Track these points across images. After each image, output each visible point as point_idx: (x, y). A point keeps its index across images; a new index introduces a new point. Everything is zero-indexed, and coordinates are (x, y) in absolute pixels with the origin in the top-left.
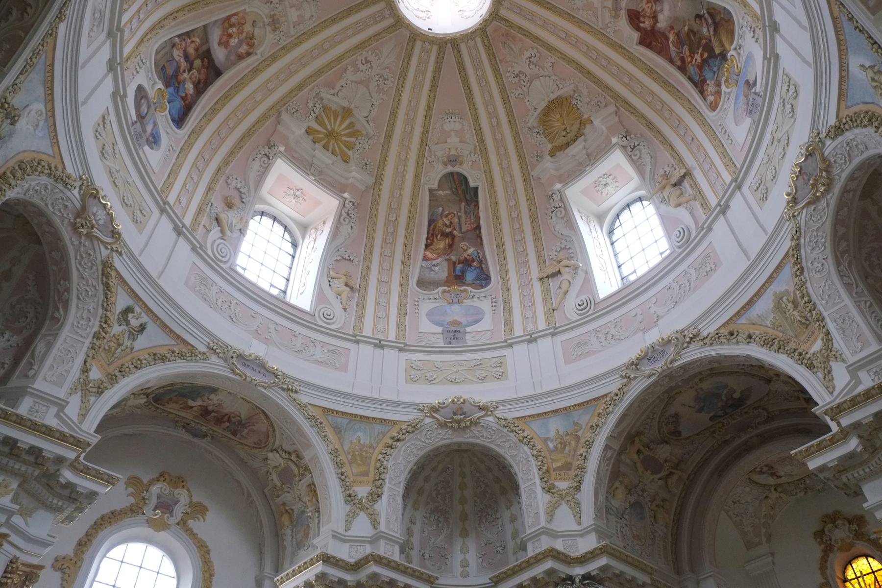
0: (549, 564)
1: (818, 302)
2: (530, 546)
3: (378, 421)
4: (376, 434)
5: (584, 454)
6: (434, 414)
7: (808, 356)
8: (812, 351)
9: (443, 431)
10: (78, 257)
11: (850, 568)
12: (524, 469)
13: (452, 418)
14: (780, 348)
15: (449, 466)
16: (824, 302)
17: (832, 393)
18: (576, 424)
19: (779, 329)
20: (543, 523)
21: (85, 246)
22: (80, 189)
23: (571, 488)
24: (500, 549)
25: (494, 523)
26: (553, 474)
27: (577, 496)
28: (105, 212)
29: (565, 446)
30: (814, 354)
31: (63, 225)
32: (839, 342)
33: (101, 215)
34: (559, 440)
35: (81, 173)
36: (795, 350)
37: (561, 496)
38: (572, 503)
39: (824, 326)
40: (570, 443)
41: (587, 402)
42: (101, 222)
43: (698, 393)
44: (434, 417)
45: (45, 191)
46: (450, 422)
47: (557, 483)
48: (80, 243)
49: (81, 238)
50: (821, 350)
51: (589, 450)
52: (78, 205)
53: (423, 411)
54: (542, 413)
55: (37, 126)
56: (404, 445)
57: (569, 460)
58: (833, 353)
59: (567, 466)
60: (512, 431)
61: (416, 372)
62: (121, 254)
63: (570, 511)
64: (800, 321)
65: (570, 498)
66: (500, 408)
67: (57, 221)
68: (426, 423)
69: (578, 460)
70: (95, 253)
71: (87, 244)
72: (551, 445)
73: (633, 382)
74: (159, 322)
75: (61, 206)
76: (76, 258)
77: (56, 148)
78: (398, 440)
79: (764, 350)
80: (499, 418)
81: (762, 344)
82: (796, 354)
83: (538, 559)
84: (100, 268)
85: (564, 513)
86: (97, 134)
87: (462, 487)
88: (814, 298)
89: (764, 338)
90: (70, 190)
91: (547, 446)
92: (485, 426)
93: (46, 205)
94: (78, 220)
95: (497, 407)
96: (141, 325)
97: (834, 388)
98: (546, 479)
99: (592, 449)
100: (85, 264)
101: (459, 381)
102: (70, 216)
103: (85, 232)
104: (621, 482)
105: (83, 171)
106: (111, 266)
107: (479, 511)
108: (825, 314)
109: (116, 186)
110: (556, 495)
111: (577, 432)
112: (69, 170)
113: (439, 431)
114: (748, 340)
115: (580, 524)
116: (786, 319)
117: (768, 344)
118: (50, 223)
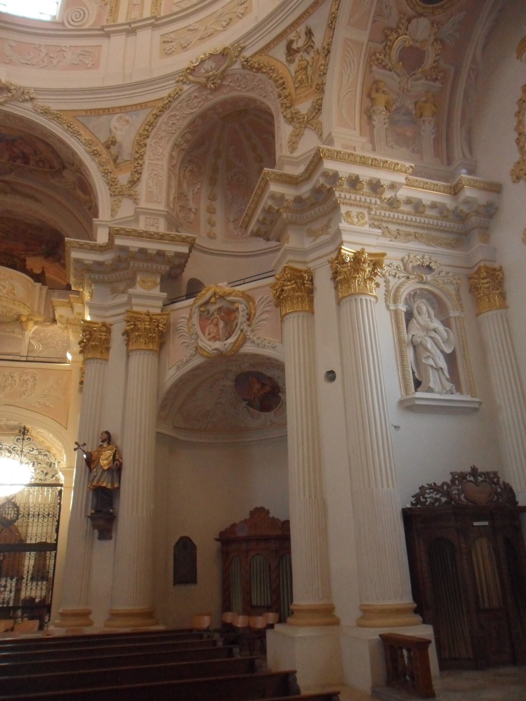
10: (239, 89)
21: (231, 82)
22: (184, 83)
28: (207, 61)
31: (212, 99)
33: (209, 65)
35: (174, 81)
42: (213, 65)
45: (176, 116)
48: (228, 85)
49: (224, 85)
52: (196, 87)
55: (127, 121)
62: (243, 48)
67: (208, 104)
70: (236, 74)
71: (229, 80)
74: (310, 11)
75: (195, 101)
76: (240, 91)
77: (149, 105)
84: (247, 72)
86: (168, 52)
90: (180, 95)
93: (191, 113)
94: (209, 86)
96: (306, 34)
100: (244, 84)
102: (204, 93)
103: (219, 81)
105: (172, 80)
106: (247, 61)
109: (212, 34)
112: (165, 94)
118: (213, 108)
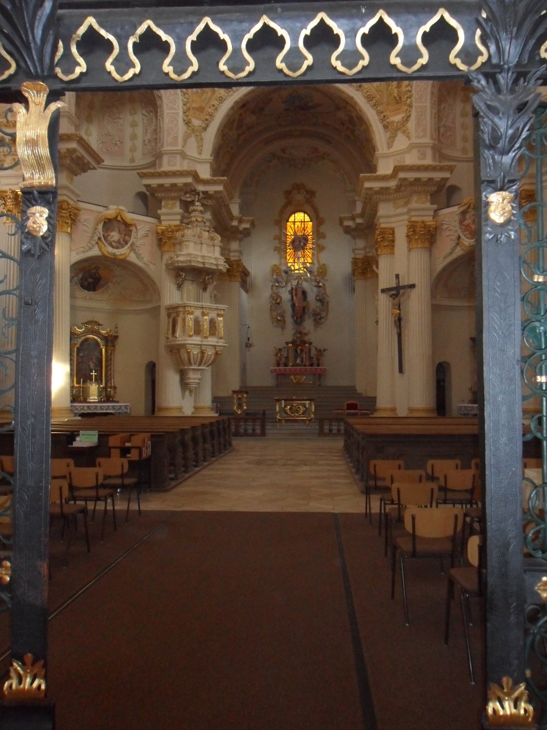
0: (189, 180)
1: (414, 95)
2: (165, 158)
5: (216, 106)
7: (388, 120)
8: (392, 119)
11: (293, 216)
12: (171, 98)
14: (375, 105)
16: (417, 97)
17: (389, 148)
19: (380, 93)
20: (179, 147)
23: (200, 126)
24: (118, 143)
25: (115, 121)
26: (192, 112)
27: (203, 134)
30: (392, 122)
32: (411, 125)
36: (382, 112)
37: (193, 130)
38: (199, 138)
39: (409, 111)
50: (398, 122)
51: (220, 104)
58: (404, 128)
59: (201, 109)
64: (395, 97)
65: (198, 134)
69: (210, 107)
79: (364, 100)
81: (366, 95)
82: (382, 115)
83: (181, 174)
85: (192, 142)
88: (413, 91)
89: (368, 93)
97: (392, 146)
98: (187, 114)
99: (222, 104)
108: (414, 104)
110: (190, 128)
114: (358, 88)
115: (200, 154)
116: (387, 90)
117: (369, 98)
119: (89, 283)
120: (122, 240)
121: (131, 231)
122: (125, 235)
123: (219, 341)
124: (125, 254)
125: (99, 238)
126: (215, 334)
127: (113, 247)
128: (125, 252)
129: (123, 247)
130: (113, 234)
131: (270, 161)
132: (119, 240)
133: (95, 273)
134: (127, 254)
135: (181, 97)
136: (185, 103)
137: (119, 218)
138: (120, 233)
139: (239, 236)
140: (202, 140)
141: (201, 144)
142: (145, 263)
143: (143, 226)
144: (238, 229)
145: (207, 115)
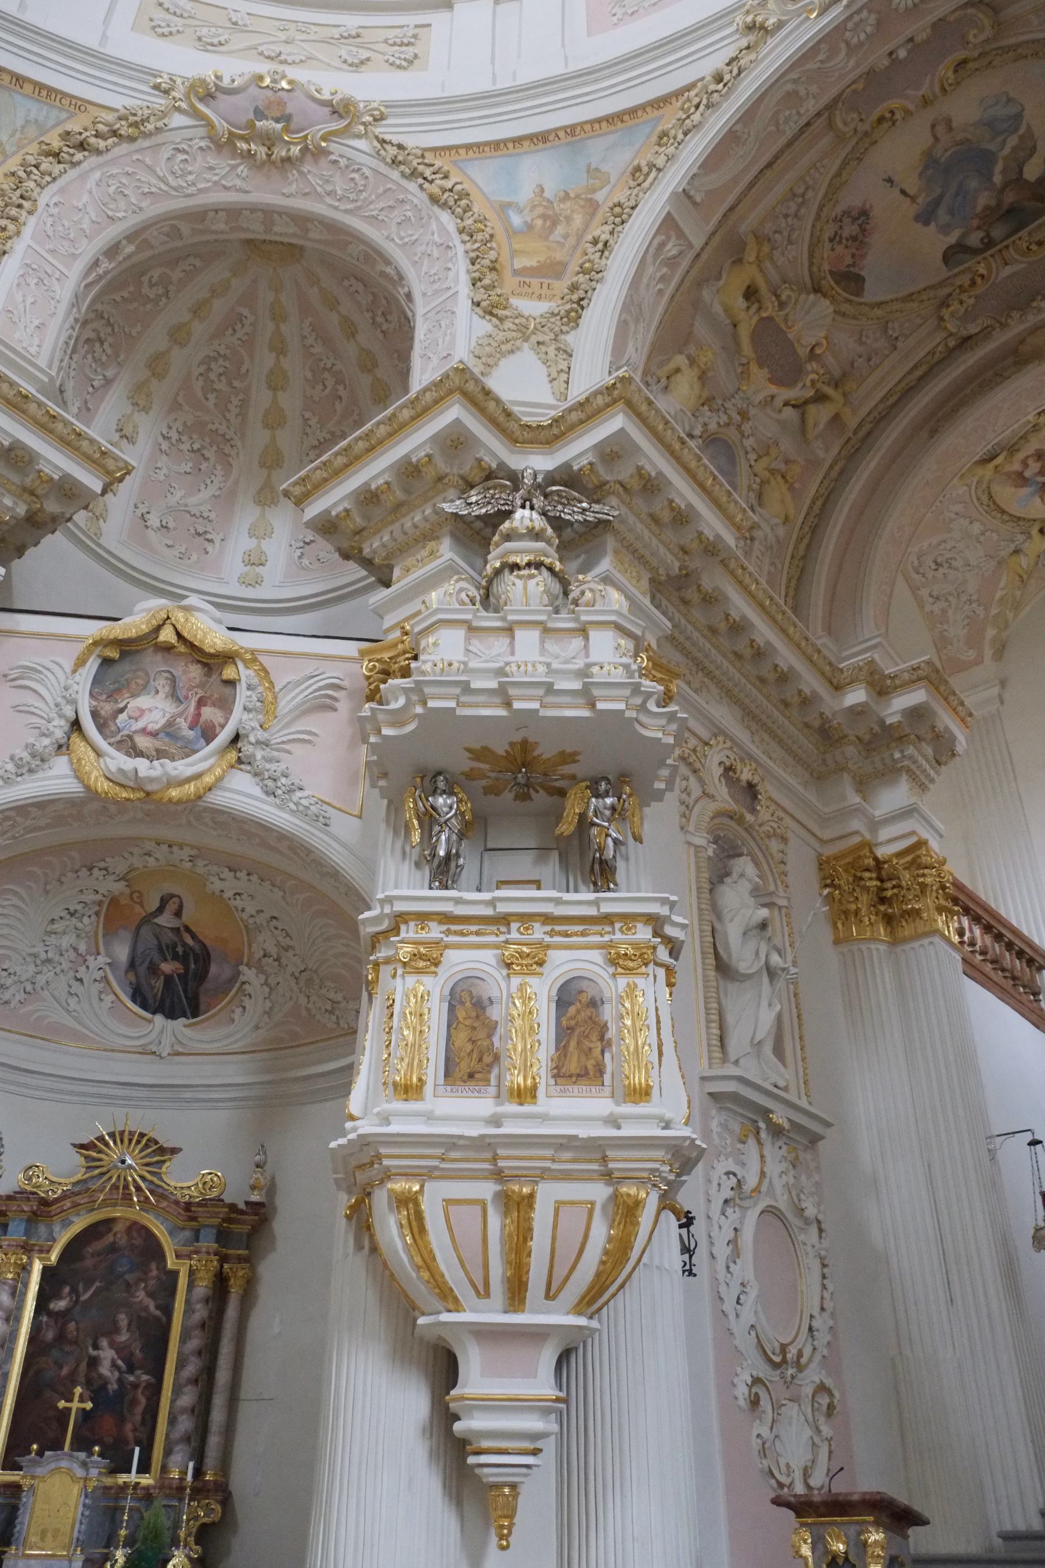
3: (28, 88)
4: (20, 122)
6: (201, 107)
9: (223, 163)
13: (251, 125)
15: (245, 312)
18: (593, 172)
23: (553, 314)
27: (570, 339)
29: (555, 223)
34: (540, 210)
38: (551, 350)
40: (568, 219)
41: (632, 112)
43: (936, 139)
44: (196, 114)
46: (242, 138)
47: (514, 301)
51: (620, 228)
53: (166, 92)
54: (506, 141)
56: (99, 166)
57: (559, 256)
59: (553, 270)
60: (414, 174)
61: (168, 17)
63: (544, 370)
66: (389, 121)
68: (173, 125)
72: (516, 220)
73: (771, 42)
78: (82, 146)
80: (383, 142)
87: (276, 382)
91: (506, 221)
92: (343, 162)
95: (382, 118)
98: (487, 281)
99: (627, 226)
101: (290, 59)
104: (692, 361)
107: (314, 447)
110: (508, 324)
111: (594, 191)
113: (212, 161)
119: (168, 979)
120: (183, 724)
121: (231, 683)
122: (201, 703)
123: (628, 1109)
124: (198, 776)
125: (76, 725)
126: (600, 1071)
127: (137, 753)
128: (190, 771)
129: (189, 750)
130: (143, 701)
131: (1017, 552)
132: (170, 724)
133: (178, 929)
134: (209, 779)
135: (460, 249)
136: (473, 255)
137: (167, 635)
138: (174, 695)
139: (897, 755)
140: (571, 356)
141: (563, 365)
142: (303, 812)
143: (308, 672)
144: (882, 722)
145: (578, 273)
